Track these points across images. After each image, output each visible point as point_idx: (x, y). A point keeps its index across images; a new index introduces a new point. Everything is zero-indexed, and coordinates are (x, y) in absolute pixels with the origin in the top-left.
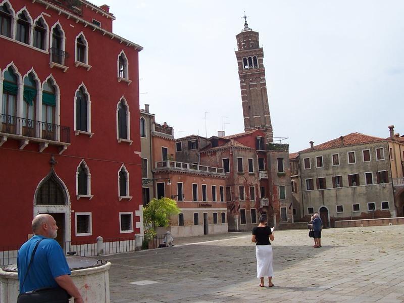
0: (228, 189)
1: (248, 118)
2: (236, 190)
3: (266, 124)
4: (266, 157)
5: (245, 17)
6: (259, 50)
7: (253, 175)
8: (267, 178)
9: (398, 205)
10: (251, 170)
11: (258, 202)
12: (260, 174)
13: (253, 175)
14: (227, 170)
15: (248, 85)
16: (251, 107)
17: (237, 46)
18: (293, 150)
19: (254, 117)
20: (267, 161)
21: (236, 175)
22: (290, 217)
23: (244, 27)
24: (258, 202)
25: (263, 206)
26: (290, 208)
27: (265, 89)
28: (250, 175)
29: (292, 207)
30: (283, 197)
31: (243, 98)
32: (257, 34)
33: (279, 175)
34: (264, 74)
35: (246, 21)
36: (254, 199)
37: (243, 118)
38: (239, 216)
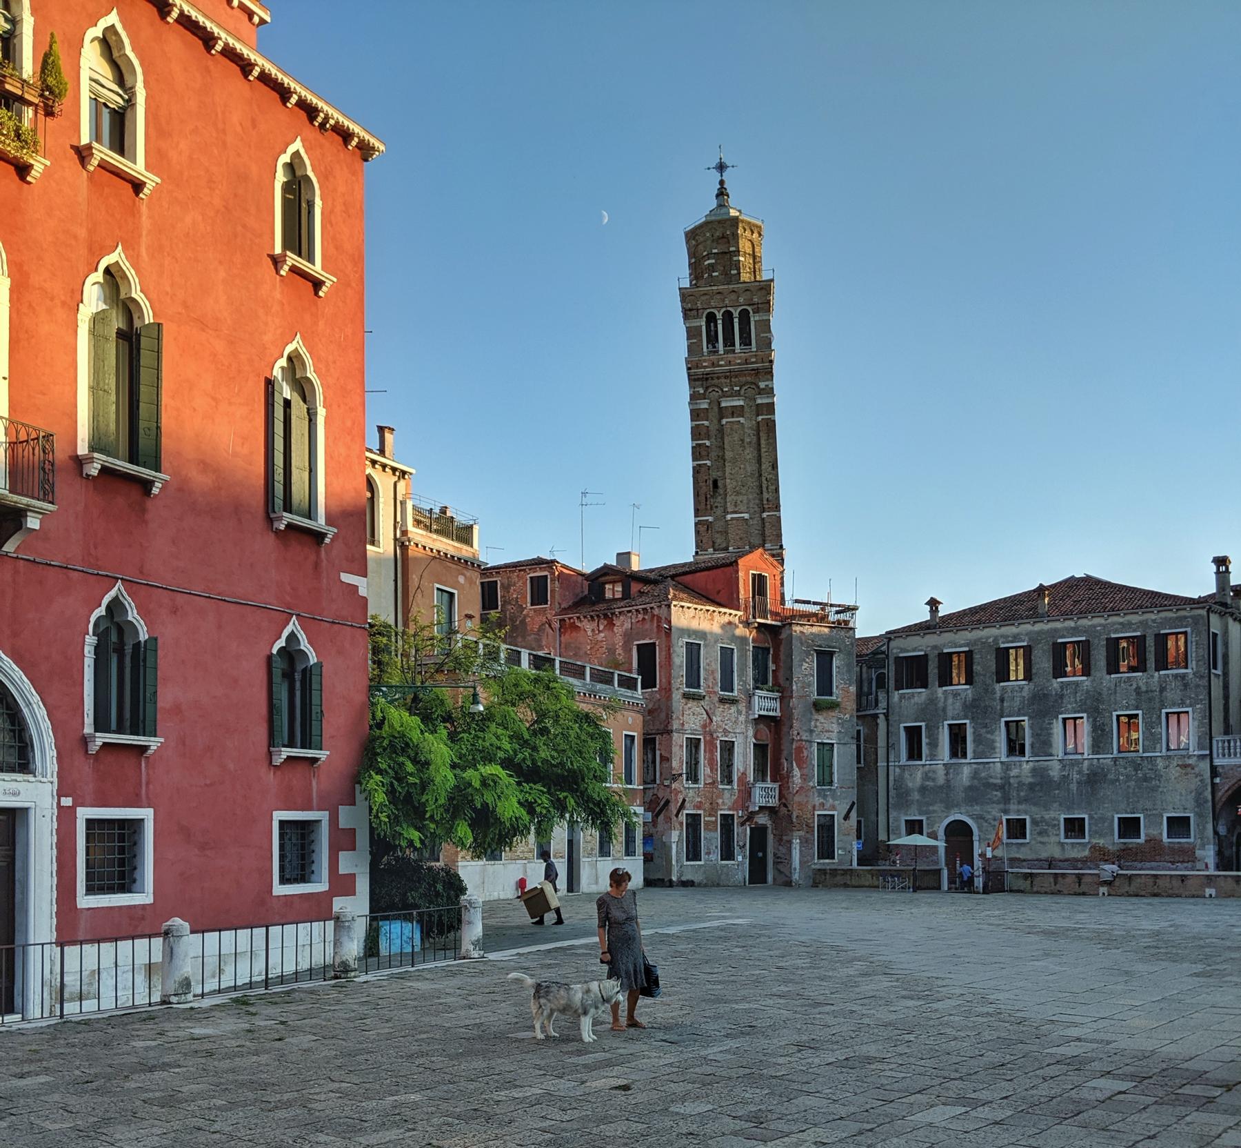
0: (649, 743)
2: (675, 749)
4: (777, 643)
7: (733, 701)
8: (778, 714)
9: (1222, 830)
10: (727, 685)
11: (746, 793)
13: (733, 701)
14: (649, 683)
15: (716, 409)
16: (720, 484)
17: (688, 272)
18: (867, 626)
19: (729, 517)
20: (782, 657)
21: (677, 696)
22: (847, 847)
24: (746, 793)
25: (760, 807)
27: (771, 426)
28: (723, 701)
30: (826, 779)
31: (697, 453)
36: (730, 782)
37: (691, 520)
38: (681, 834)
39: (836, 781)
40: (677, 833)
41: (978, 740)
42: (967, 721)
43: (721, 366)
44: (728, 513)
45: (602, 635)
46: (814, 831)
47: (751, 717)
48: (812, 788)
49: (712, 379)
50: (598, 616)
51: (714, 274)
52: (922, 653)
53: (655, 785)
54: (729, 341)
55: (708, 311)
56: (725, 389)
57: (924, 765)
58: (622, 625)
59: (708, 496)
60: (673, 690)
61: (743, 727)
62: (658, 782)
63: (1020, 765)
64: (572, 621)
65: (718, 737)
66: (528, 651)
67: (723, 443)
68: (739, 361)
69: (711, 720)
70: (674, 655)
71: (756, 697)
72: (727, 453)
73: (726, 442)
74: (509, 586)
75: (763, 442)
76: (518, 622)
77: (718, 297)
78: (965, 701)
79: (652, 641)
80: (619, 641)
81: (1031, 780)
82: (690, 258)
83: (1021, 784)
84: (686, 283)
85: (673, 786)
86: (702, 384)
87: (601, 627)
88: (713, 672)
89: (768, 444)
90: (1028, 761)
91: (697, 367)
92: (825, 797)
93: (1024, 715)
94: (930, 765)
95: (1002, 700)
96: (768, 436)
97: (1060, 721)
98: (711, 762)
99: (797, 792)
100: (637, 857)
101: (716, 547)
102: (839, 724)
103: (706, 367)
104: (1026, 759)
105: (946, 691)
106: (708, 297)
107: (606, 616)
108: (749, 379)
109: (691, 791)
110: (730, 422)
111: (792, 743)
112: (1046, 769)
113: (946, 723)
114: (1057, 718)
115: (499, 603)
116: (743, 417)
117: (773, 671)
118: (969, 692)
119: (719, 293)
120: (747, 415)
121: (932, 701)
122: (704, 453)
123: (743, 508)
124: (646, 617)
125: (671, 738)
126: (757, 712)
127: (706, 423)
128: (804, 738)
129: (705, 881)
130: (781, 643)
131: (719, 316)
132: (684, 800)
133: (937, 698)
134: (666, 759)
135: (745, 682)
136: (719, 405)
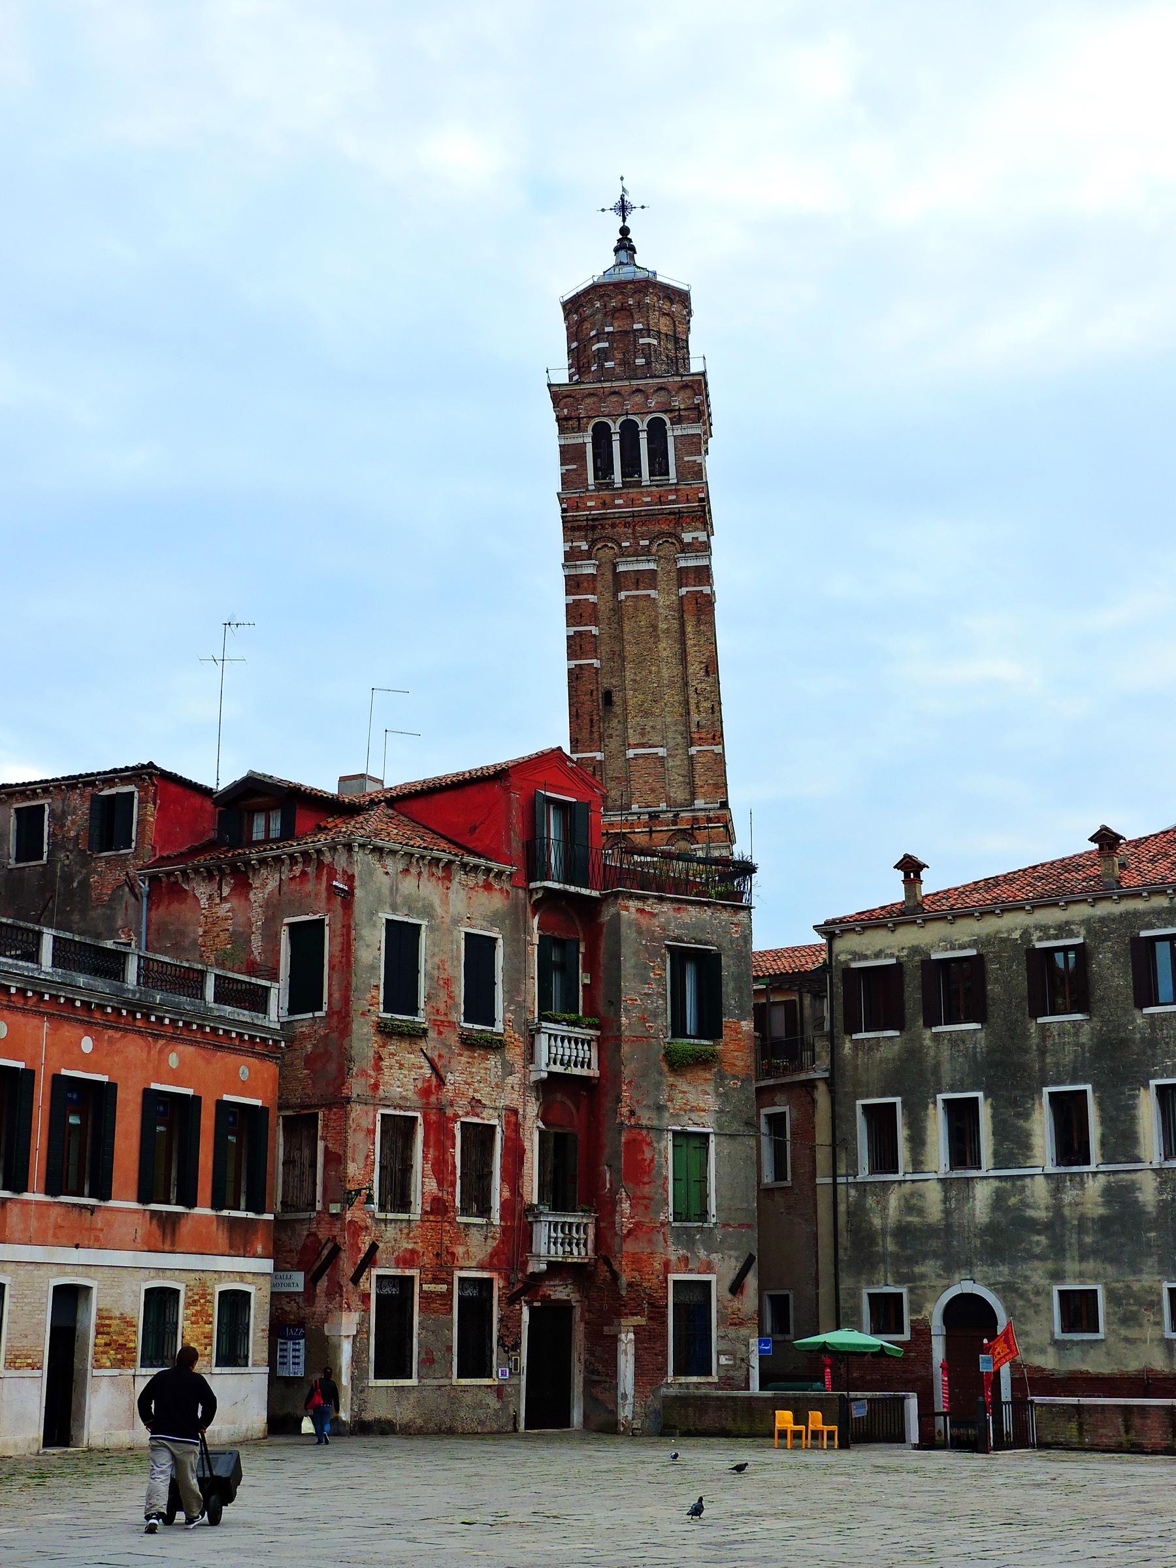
1: (599, 756)
2: (356, 1139)
3: (693, 795)
4: (594, 932)
5: (623, 208)
6: (685, 386)
7: (494, 1045)
8: (594, 1072)
12: (543, 1041)
15: (609, 576)
16: (616, 698)
19: (631, 753)
20: (603, 958)
23: (611, 260)
25: (549, 1263)
26: (736, 1288)
27: (704, 606)
28: (469, 1043)
29: (751, 1281)
31: (576, 647)
32: (681, 298)
33: (679, 1063)
34: (701, 516)
35: (624, 231)
36: (485, 1210)
38: (363, 1321)
39: (713, 1211)
40: (355, 1317)
41: (1001, 1131)
42: (980, 1095)
43: (619, 506)
44: (630, 746)
45: (228, 905)
46: (665, 1315)
47: (534, 1077)
48: (663, 1224)
49: (603, 527)
50: (220, 869)
51: (609, 364)
52: (893, 961)
53: (314, 1214)
54: (631, 465)
55: (597, 420)
56: (624, 544)
57: (900, 1182)
58: (264, 885)
59: (596, 718)
60: (353, 1013)
61: (515, 1096)
62: (319, 1207)
63: (1082, 1183)
64: (172, 879)
65: (456, 1116)
66: (53, 932)
67: (622, 632)
68: (649, 499)
69: (441, 1081)
70: (355, 945)
71: (544, 1038)
72: (627, 647)
73: (626, 629)
74: (64, 813)
75: (689, 629)
76: (75, 885)
77: (614, 399)
78: (975, 1054)
79: (316, 917)
80: (257, 917)
81: (1101, 1211)
82: (570, 340)
83: (1082, 1218)
84: (562, 377)
85: (349, 1216)
86: (586, 536)
87: (226, 891)
88: (448, 982)
89: (698, 632)
90: (1095, 1174)
91: (577, 509)
92: (690, 1244)
93: (1086, 1082)
94: (913, 1181)
95: (1042, 1052)
96: (699, 620)
97: (1153, 1090)
98: (440, 1169)
99: (630, 1232)
100: (250, 1369)
101: (610, 803)
102: (718, 1095)
103: (591, 509)
104: (1092, 1168)
105: (937, 1035)
106: (595, 399)
107: (235, 871)
108: (665, 527)
109: (390, 1227)
110: (633, 596)
111: (620, 1133)
112: (1132, 1188)
113: (940, 1097)
114: (1146, 1086)
115: (45, 848)
116: (655, 589)
117: (585, 985)
118: (981, 1035)
119: (615, 393)
120: (662, 585)
121: (913, 1055)
122: (588, 647)
123: (656, 739)
124: (308, 869)
125: (346, 1116)
126: (543, 1067)
127: (592, 598)
128: (644, 1122)
129: (419, 1422)
130: (600, 932)
131: (615, 428)
132: (374, 1247)
133: (922, 1045)
134: (336, 1160)
135: (521, 1007)
136: (615, 566)
